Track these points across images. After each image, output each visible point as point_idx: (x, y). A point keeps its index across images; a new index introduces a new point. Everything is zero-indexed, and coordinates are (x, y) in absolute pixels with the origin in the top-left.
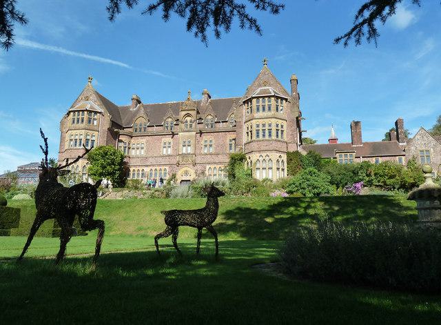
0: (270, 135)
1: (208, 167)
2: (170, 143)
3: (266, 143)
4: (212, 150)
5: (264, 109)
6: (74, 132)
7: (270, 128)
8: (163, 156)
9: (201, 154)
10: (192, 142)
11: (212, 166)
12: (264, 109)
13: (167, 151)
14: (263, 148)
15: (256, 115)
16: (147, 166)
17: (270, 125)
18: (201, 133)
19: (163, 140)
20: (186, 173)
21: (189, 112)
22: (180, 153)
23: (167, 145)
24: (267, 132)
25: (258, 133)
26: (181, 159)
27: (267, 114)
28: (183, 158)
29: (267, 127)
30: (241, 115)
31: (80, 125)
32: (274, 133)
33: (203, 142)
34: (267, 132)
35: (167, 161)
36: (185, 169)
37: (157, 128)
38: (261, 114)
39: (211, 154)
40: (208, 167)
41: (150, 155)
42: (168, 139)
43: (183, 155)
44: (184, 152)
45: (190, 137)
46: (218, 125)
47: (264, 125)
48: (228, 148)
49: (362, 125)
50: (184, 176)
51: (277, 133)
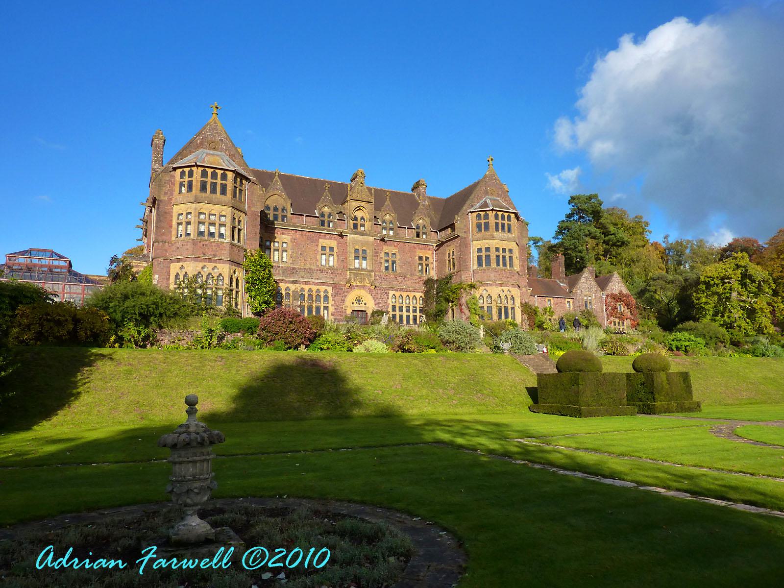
1: (391, 293)
11: (398, 294)
15: (496, 234)
16: (294, 282)
21: (363, 204)
28: (356, 275)
33: (383, 255)
38: (500, 234)
40: (391, 293)
42: (333, 244)
43: (358, 272)
44: (357, 265)
45: (363, 244)
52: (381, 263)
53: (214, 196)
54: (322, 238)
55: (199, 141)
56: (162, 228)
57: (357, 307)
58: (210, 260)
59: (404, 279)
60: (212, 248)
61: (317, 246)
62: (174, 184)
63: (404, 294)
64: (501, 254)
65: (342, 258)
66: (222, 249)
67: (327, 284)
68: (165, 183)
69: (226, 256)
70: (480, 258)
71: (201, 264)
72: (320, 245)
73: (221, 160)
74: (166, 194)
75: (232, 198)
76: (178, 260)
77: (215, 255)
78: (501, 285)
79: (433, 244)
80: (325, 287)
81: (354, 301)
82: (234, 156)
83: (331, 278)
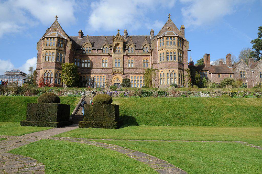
0: (175, 59)
3: (173, 63)
6: (48, 51)
7: (168, 55)
10: (121, 60)
11: (133, 75)
13: (105, 65)
14: (171, 66)
17: (175, 53)
18: (127, 55)
19: (102, 58)
24: (173, 57)
26: (114, 71)
29: (173, 54)
30: (155, 46)
34: (173, 57)
35: (105, 71)
42: (107, 58)
43: (116, 68)
47: (171, 53)
49: (211, 56)
50: (116, 81)
52: (127, 64)
56: (39, 59)
57: (116, 82)
73: (56, 34)
74: (40, 48)
80: (103, 75)
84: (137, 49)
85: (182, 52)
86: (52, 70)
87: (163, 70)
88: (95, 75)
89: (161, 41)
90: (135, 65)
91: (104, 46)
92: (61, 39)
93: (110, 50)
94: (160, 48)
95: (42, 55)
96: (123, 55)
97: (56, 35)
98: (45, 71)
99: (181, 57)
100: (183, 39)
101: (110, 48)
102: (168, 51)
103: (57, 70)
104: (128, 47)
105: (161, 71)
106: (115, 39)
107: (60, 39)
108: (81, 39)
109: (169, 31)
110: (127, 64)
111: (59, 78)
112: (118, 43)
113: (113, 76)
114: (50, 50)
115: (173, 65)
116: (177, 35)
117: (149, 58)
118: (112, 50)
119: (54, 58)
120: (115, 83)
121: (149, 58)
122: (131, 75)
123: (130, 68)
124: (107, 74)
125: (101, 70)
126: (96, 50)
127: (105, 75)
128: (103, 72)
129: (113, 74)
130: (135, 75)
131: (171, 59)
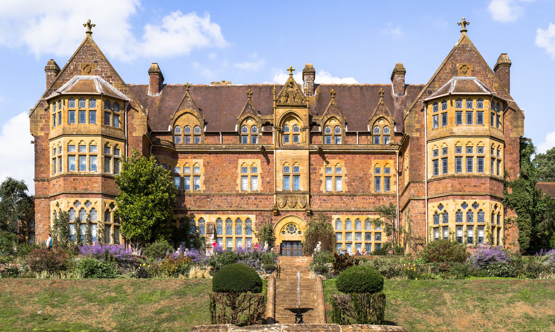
0: (481, 168)
2: (254, 169)
3: (473, 182)
4: (341, 186)
5: (469, 120)
8: (242, 195)
9: (320, 194)
10: (303, 169)
11: (343, 217)
12: (469, 120)
17: (481, 150)
18: (321, 153)
19: (241, 161)
20: (291, 227)
22: (280, 189)
23: (249, 173)
24: (475, 161)
25: (459, 163)
26: (281, 201)
27: (474, 128)
29: (475, 153)
30: (418, 126)
31: (87, 126)
32: (487, 162)
34: (475, 161)
36: (289, 220)
37: (225, 137)
38: (463, 128)
39: (340, 195)
41: (215, 188)
42: (258, 162)
43: (286, 194)
46: (350, 139)
47: (469, 149)
48: (373, 185)
51: (492, 164)
52: (321, 181)
53: (82, 125)
54: (241, 158)
55: (72, 67)
58: (82, 195)
59: (353, 199)
60: (83, 183)
61: (236, 168)
62: (49, 118)
63: (353, 218)
64: (464, 153)
65: (268, 179)
66: (94, 182)
67: (251, 211)
68: (41, 118)
69: (97, 187)
70: (435, 161)
71: (73, 200)
72: (239, 166)
73: (99, 84)
75: (102, 126)
76: (55, 197)
77: (86, 189)
78: (462, 196)
79: (396, 151)
81: (285, 230)
82: (111, 77)
83: (255, 204)
84: (354, 134)
85: (502, 145)
86: (92, 200)
87: (444, 203)
88: (218, 216)
89: (436, 109)
90: (349, 184)
91: (243, 121)
92: (112, 102)
93: (265, 134)
94: (433, 134)
95: (51, 150)
96: (310, 153)
97: (99, 90)
98: (71, 205)
99: (499, 161)
100: (505, 103)
101: (263, 129)
102: (459, 144)
103: (109, 201)
104: (321, 124)
105: (436, 204)
106: (282, 100)
107: (111, 102)
108: (157, 95)
109: (463, 78)
110: (321, 181)
111: (115, 226)
112: (291, 113)
113: (279, 218)
114: (79, 139)
115: (475, 186)
116: (489, 93)
117: (391, 162)
118: (271, 134)
119: (98, 162)
120: (283, 241)
121: (392, 163)
122: (335, 217)
123: (331, 194)
124: (259, 212)
125: (239, 199)
126: (217, 134)
127: (253, 217)
128: (246, 207)
129: (278, 213)
130: (350, 216)
131: (470, 168)
